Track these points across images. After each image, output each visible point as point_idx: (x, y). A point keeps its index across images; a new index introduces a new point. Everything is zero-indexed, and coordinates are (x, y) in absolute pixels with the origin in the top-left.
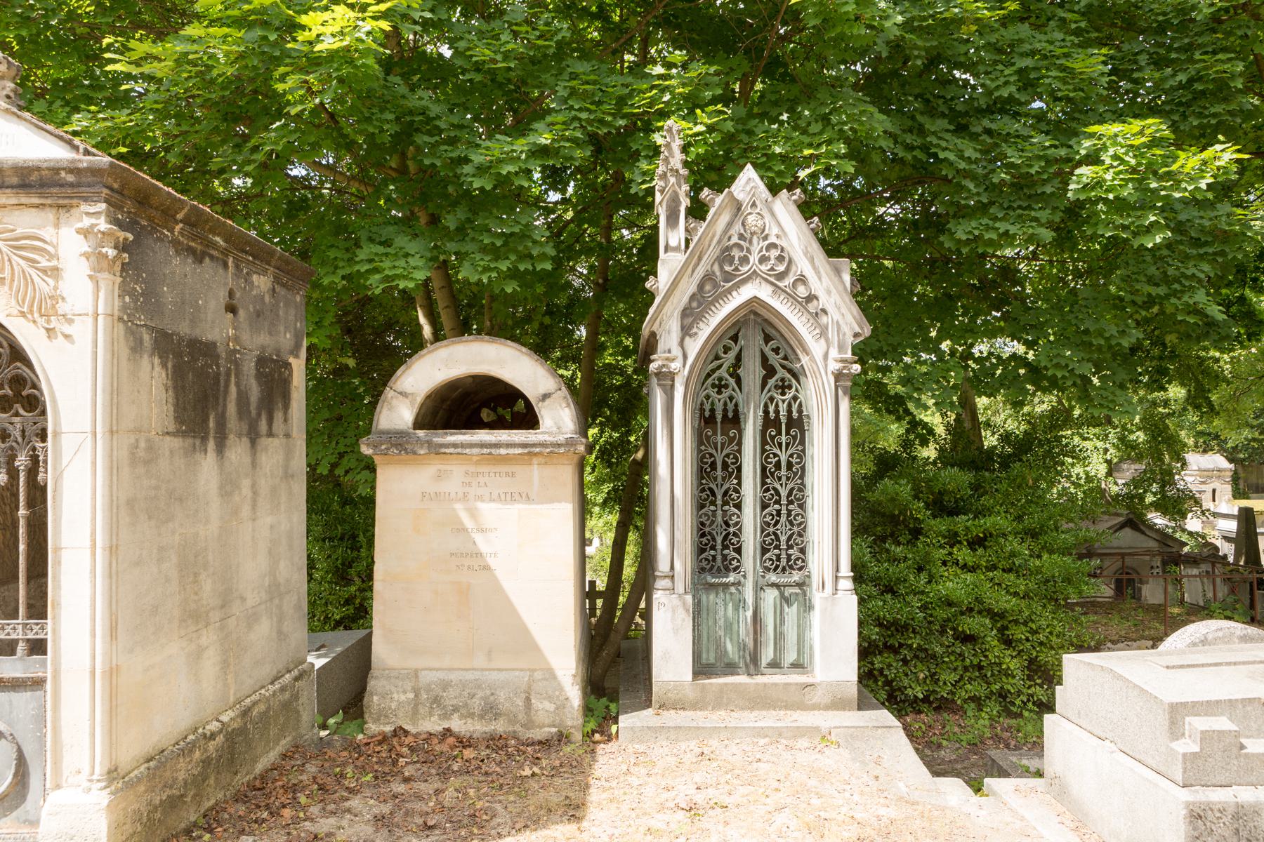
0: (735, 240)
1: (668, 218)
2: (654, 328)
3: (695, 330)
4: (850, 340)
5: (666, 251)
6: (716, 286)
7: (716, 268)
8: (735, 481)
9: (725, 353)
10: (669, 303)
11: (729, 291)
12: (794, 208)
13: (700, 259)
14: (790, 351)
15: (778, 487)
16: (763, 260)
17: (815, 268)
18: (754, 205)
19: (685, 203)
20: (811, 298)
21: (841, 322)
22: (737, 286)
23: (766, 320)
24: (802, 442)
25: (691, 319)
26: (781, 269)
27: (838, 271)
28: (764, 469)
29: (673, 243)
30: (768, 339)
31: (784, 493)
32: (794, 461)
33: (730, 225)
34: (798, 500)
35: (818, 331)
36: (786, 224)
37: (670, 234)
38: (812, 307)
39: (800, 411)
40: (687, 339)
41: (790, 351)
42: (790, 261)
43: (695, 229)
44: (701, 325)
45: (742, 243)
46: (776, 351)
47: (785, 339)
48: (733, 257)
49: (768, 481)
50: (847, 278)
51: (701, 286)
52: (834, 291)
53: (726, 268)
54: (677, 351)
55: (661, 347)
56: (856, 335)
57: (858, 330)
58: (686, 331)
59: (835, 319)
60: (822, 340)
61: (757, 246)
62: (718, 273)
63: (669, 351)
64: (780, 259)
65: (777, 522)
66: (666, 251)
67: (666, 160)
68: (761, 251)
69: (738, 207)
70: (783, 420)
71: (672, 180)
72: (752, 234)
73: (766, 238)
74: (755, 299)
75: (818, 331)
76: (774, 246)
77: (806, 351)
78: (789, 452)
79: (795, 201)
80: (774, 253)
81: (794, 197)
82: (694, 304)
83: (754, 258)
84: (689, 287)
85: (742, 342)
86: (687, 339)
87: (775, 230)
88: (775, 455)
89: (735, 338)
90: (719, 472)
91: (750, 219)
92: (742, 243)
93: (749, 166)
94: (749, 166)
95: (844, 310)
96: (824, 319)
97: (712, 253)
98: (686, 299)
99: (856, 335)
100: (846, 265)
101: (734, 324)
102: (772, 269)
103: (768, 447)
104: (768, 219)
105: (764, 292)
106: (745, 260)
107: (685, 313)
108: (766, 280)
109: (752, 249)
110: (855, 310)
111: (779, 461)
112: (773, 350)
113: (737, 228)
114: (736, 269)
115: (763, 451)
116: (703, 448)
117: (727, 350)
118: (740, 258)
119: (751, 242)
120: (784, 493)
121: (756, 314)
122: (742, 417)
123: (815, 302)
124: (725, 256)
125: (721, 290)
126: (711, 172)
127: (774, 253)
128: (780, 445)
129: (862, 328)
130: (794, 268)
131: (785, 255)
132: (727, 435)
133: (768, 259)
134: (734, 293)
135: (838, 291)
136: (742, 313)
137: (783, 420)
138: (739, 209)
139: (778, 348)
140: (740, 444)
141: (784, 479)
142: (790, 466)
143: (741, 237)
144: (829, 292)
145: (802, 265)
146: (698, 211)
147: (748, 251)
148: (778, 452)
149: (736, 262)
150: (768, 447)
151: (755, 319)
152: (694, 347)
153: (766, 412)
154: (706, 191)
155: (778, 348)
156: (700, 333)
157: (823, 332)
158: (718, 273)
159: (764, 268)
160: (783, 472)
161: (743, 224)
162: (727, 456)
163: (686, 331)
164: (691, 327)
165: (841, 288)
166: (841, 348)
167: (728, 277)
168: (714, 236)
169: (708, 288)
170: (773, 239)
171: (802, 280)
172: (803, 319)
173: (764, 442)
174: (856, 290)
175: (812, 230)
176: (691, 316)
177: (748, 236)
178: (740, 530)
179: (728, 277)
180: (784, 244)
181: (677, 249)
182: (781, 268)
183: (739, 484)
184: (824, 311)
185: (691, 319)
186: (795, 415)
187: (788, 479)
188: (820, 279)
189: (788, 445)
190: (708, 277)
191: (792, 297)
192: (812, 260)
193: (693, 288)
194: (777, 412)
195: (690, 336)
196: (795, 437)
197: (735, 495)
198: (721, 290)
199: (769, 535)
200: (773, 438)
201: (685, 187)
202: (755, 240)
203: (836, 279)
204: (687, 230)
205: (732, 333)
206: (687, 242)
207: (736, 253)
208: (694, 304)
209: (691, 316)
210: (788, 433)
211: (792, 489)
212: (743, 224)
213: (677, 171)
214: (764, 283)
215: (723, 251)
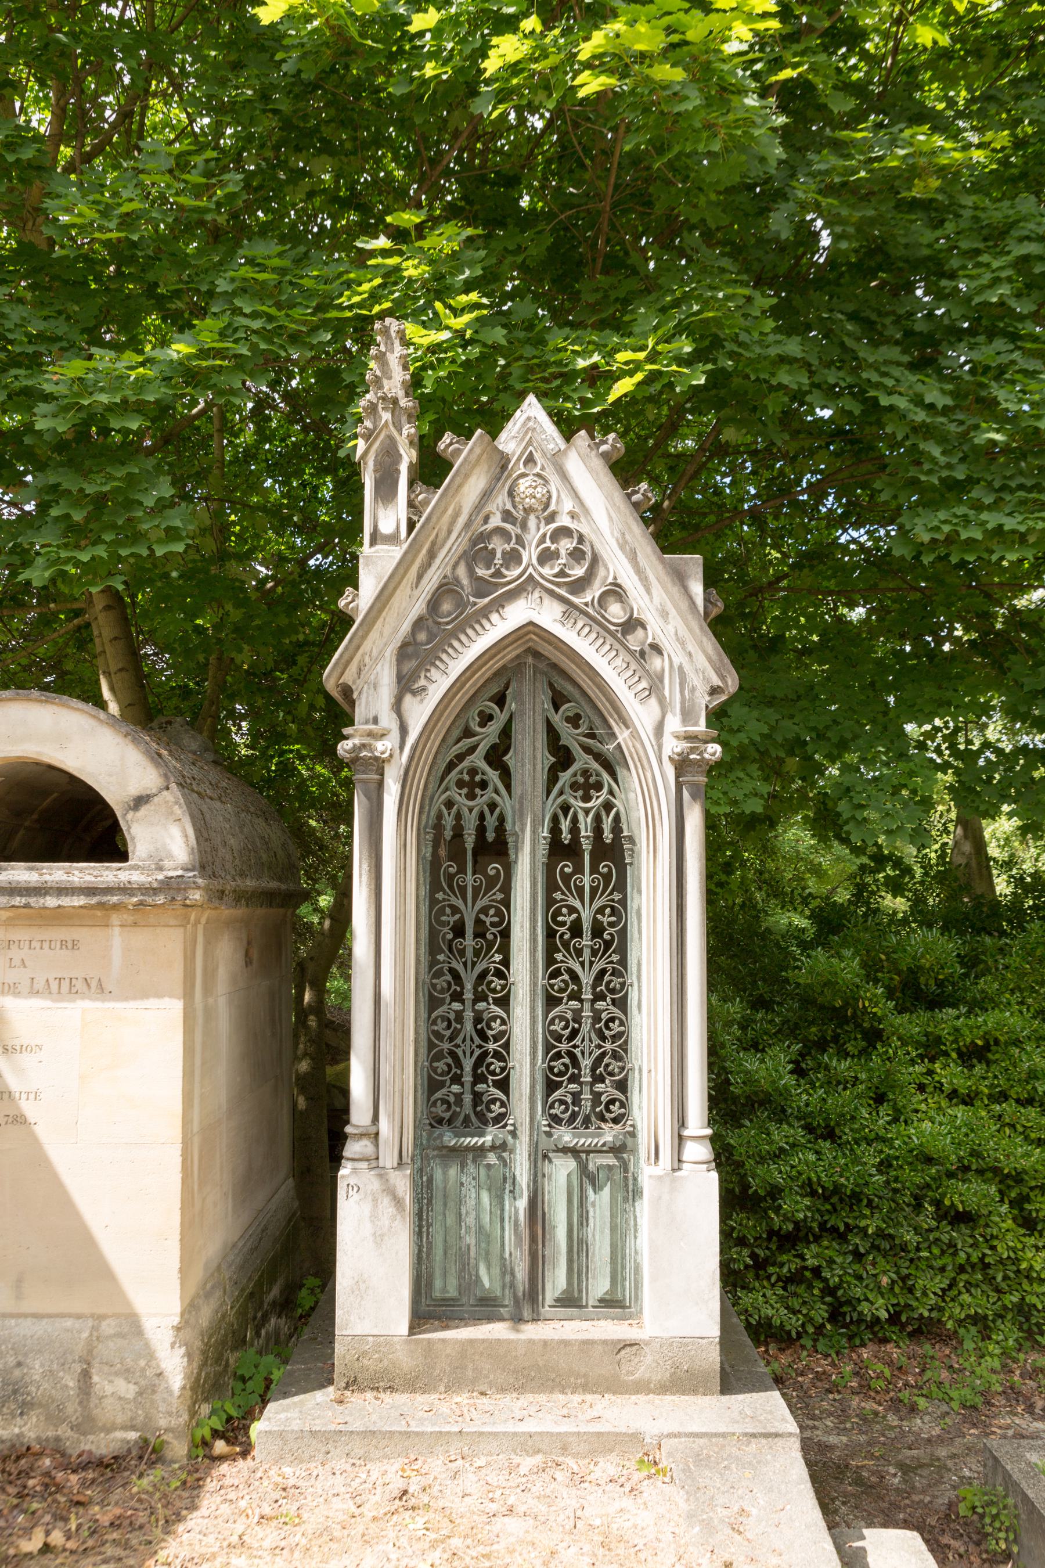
0: (496, 521)
1: (378, 484)
2: (348, 677)
3: (422, 682)
4: (703, 700)
5: (373, 542)
6: (461, 604)
7: (462, 571)
8: (498, 957)
9: (482, 725)
10: (374, 635)
11: (485, 613)
12: (598, 464)
13: (432, 555)
14: (597, 721)
15: (577, 968)
16: (546, 557)
17: (639, 571)
18: (530, 460)
19: (408, 456)
20: (632, 624)
21: (687, 667)
22: (499, 604)
23: (554, 666)
24: (621, 886)
25: (413, 663)
26: (578, 575)
27: (680, 578)
28: (550, 934)
29: (386, 527)
30: (558, 700)
31: (587, 979)
32: (605, 920)
33: (486, 495)
34: (613, 991)
35: (644, 684)
36: (585, 492)
37: (381, 513)
38: (634, 640)
39: (617, 829)
40: (408, 698)
41: (597, 721)
42: (595, 559)
43: (426, 502)
44: (434, 673)
45: (508, 526)
46: (574, 721)
47: (590, 700)
48: (493, 552)
49: (559, 957)
50: (697, 588)
51: (434, 605)
52: (673, 612)
53: (482, 572)
54: (388, 721)
55: (360, 713)
56: (714, 691)
57: (716, 681)
58: (406, 685)
59: (676, 661)
60: (653, 701)
61: (535, 532)
62: (465, 582)
63: (375, 721)
64: (577, 555)
65: (574, 1033)
66: (373, 542)
67: (378, 381)
68: (542, 540)
69: (503, 463)
70: (586, 845)
71: (386, 416)
72: (528, 511)
73: (551, 518)
74: (531, 628)
75: (644, 684)
76: (564, 532)
77: (625, 722)
78: (598, 904)
79: (605, 455)
80: (566, 545)
81: (604, 448)
82: (422, 637)
83: (530, 555)
84: (410, 604)
85: (512, 705)
86: (408, 698)
87: (568, 505)
88: (572, 910)
89: (500, 700)
90: (469, 942)
91: (523, 485)
92: (508, 526)
93: (531, 398)
94: (531, 398)
95: (692, 647)
96: (656, 663)
97: (454, 545)
98: (406, 627)
99: (714, 691)
100: (694, 563)
101: (497, 674)
102: (562, 574)
103: (558, 895)
104: (555, 483)
105: (548, 615)
106: (513, 558)
107: (406, 651)
108: (552, 593)
109: (527, 538)
110: (710, 644)
111: (579, 920)
112: (568, 720)
113: (501, 500)
114: (498, 574)
115: (550, 902)
116: (440, 896)
117: (486, 719)
118: (504, 553)
119: (524, 526)
120: (587, 979)
121: (537, 655)
122: (510, 840)
123: (640, 632)
124: (478, 551)
125: (469, 610)
126: (461, 406)
127: (566, 545)
128: (580, 891)
129: (722, 678)
130: (601, 572)
131: (586, 548)
132: (485, 874)
133: (556, 555)
134: (494, 617)
135: (679, 612)
136: (511, 654)
137: (586, 845)
138: (504, 468)
139: (578, 717)
140: (507, 889)
141: (587, 954)
142: (597, 931)
143: (507, 516)
144: (664, 614)
145: (617, 566)
146: (432, 470)
147: (520, 541)
148: (577, 904)
149: (498, 561)
150: (558, 895)
151: (533, 659)
152: (419, 712)
153: (555, 830)
154: (448, 437)
155: (578, 717)
156: (432, 688)
157: (655, 687)
158: (465, 582)
159: (547, 571)
160: (586, 941)
161: (511, 494)
162: (484, 910)
163: (406, 685)
164: (414, 676)
165: (684, 605)
166: (687, 715)
167: (482, 587)
168: (457, 515)
169: (446, 606)
170: (564, 520)
171: (616, 592)
172: (618, 662)
173: (551, 887)
174: (715, 612)
175: (636, 505)
176: (415, 658)
177: (519, 515)
178: (507, 1046)
179: (482, 587)
180: (584, 529)
181: (393, 539)
182: (579, 572)
183: (506, 962)
184: (656, 648)
185: (413, 663)
186: (608, 836)
187: (594, 953)
188: (648, 591)
189: (594, 891)
190: (446, 589)
191: (598, 624)
192: (633, 557)
193: (419, 608)
194: (574, 830)
195: (414, 693)
196: (607, 878)
197: (497, 983)
198: (469, 610)
199: (558, 1056)
200: (450, 878)
201: (409, 429)
202: (532, 522)
203: (675, 590)
204: (411, 504)
205: (494, 689)
206: (411, 525)
207: (499, 546)
208: (422, 637)
209: (415, 658)
210: (594, 870)
211: (603, 972)
212: (511, 494)
213: (395, 401)
214: (547, 600)
215: (474, 542)
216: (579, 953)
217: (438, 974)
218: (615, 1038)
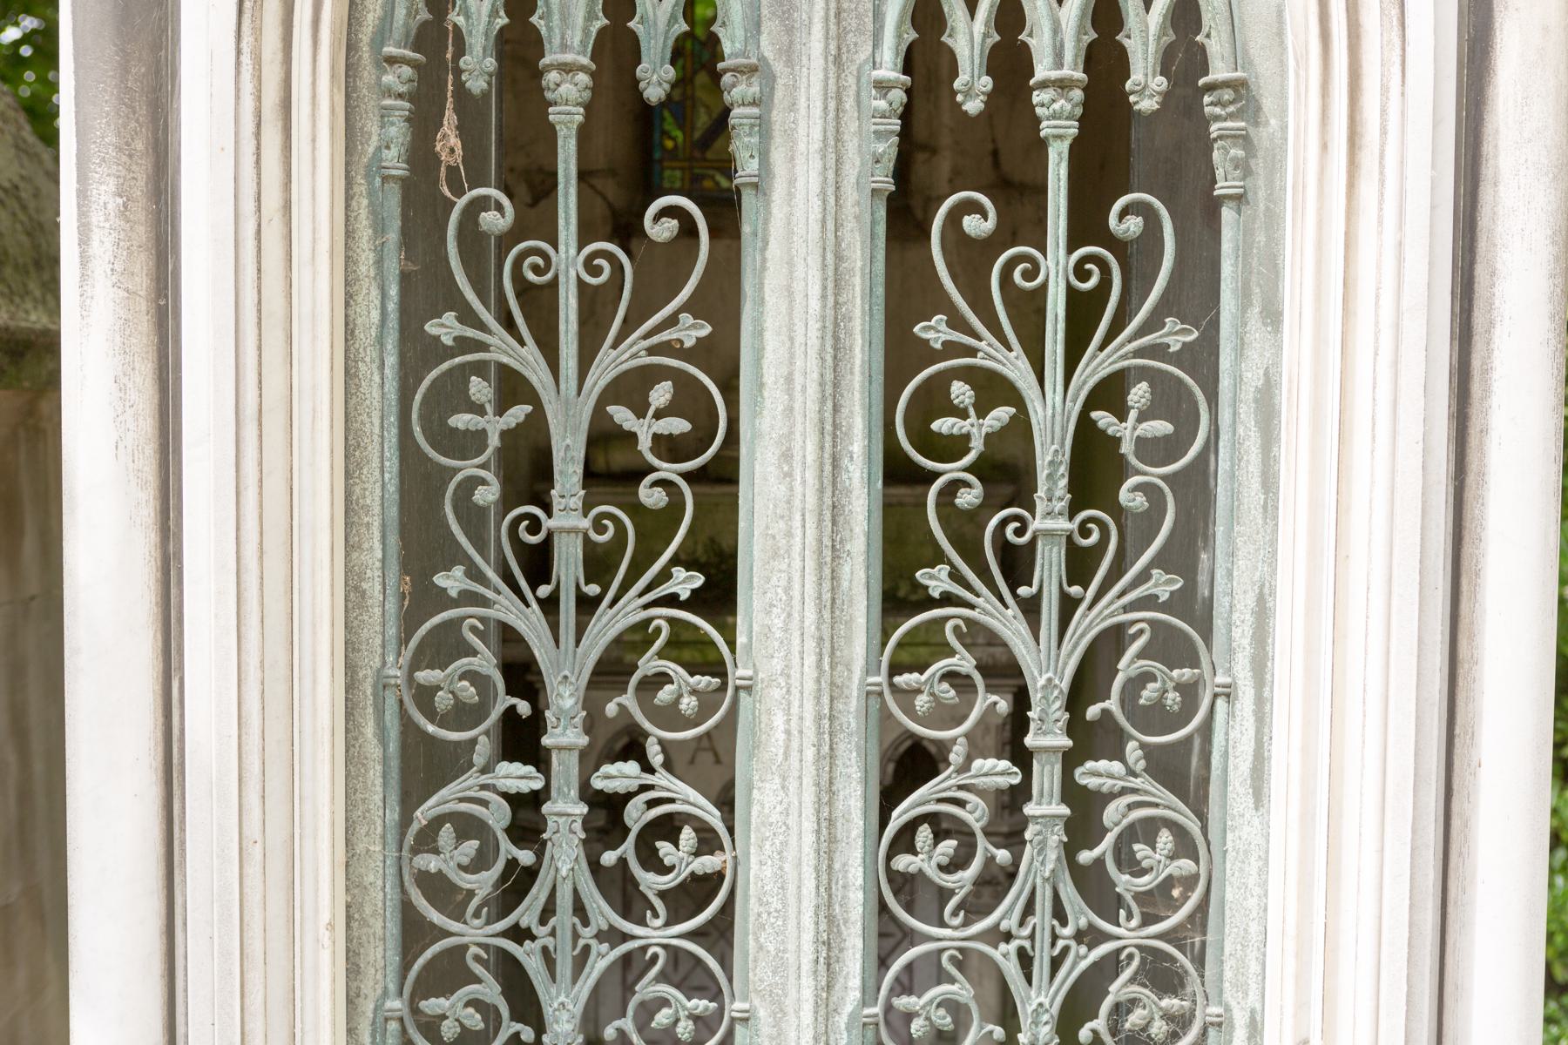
8: (685, 582)
15: (1008, 624)
24: (1197, 294)
31: (1048, 670)
32: (1127, 432)
34: (1155, 718)
39: (1184, 57)
49: (936, 580)
70: (1057, 118)
88: (993, 389)
103: (935, 331)
111: (1021, 426)
115: (902, 353)
116: (445, 328)
120: (1048, 670)
122: (738, 91)
128: (1029, 309)
132: (626, 230)
137: (1057, 118)
140: (722, 300)
141: (1049, 567)
142: (1094, 466)
148: (1016, 367)
150: (935, 331)
153: (926, 61)
160: (1049, 517)
162: (631, 389)
173: (906, 295)
178: (720, 934)
183: (719, 597)
186: (1146, 85)
187: (1080, 564)
189: (1083, 312)
194: (1010, 61)
196: (1136, 258)
197: (684, 689)
200: (971, 259)
210: (1087, 224)
211: (1112, 641)
216: (1016, 563)
217: (444, 648)
218: (1155, 903)
